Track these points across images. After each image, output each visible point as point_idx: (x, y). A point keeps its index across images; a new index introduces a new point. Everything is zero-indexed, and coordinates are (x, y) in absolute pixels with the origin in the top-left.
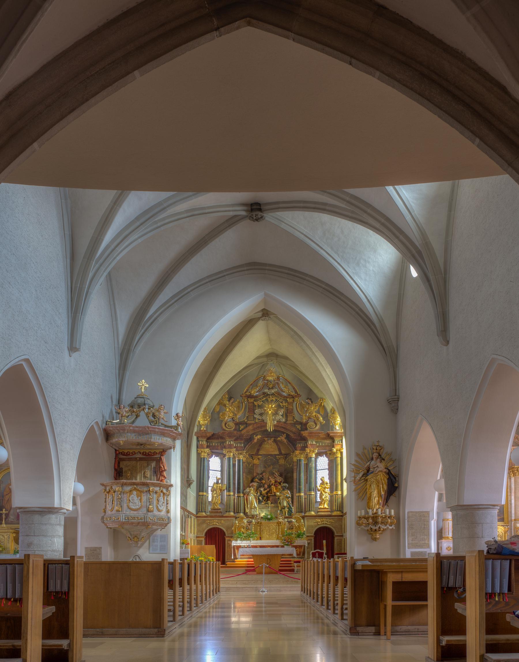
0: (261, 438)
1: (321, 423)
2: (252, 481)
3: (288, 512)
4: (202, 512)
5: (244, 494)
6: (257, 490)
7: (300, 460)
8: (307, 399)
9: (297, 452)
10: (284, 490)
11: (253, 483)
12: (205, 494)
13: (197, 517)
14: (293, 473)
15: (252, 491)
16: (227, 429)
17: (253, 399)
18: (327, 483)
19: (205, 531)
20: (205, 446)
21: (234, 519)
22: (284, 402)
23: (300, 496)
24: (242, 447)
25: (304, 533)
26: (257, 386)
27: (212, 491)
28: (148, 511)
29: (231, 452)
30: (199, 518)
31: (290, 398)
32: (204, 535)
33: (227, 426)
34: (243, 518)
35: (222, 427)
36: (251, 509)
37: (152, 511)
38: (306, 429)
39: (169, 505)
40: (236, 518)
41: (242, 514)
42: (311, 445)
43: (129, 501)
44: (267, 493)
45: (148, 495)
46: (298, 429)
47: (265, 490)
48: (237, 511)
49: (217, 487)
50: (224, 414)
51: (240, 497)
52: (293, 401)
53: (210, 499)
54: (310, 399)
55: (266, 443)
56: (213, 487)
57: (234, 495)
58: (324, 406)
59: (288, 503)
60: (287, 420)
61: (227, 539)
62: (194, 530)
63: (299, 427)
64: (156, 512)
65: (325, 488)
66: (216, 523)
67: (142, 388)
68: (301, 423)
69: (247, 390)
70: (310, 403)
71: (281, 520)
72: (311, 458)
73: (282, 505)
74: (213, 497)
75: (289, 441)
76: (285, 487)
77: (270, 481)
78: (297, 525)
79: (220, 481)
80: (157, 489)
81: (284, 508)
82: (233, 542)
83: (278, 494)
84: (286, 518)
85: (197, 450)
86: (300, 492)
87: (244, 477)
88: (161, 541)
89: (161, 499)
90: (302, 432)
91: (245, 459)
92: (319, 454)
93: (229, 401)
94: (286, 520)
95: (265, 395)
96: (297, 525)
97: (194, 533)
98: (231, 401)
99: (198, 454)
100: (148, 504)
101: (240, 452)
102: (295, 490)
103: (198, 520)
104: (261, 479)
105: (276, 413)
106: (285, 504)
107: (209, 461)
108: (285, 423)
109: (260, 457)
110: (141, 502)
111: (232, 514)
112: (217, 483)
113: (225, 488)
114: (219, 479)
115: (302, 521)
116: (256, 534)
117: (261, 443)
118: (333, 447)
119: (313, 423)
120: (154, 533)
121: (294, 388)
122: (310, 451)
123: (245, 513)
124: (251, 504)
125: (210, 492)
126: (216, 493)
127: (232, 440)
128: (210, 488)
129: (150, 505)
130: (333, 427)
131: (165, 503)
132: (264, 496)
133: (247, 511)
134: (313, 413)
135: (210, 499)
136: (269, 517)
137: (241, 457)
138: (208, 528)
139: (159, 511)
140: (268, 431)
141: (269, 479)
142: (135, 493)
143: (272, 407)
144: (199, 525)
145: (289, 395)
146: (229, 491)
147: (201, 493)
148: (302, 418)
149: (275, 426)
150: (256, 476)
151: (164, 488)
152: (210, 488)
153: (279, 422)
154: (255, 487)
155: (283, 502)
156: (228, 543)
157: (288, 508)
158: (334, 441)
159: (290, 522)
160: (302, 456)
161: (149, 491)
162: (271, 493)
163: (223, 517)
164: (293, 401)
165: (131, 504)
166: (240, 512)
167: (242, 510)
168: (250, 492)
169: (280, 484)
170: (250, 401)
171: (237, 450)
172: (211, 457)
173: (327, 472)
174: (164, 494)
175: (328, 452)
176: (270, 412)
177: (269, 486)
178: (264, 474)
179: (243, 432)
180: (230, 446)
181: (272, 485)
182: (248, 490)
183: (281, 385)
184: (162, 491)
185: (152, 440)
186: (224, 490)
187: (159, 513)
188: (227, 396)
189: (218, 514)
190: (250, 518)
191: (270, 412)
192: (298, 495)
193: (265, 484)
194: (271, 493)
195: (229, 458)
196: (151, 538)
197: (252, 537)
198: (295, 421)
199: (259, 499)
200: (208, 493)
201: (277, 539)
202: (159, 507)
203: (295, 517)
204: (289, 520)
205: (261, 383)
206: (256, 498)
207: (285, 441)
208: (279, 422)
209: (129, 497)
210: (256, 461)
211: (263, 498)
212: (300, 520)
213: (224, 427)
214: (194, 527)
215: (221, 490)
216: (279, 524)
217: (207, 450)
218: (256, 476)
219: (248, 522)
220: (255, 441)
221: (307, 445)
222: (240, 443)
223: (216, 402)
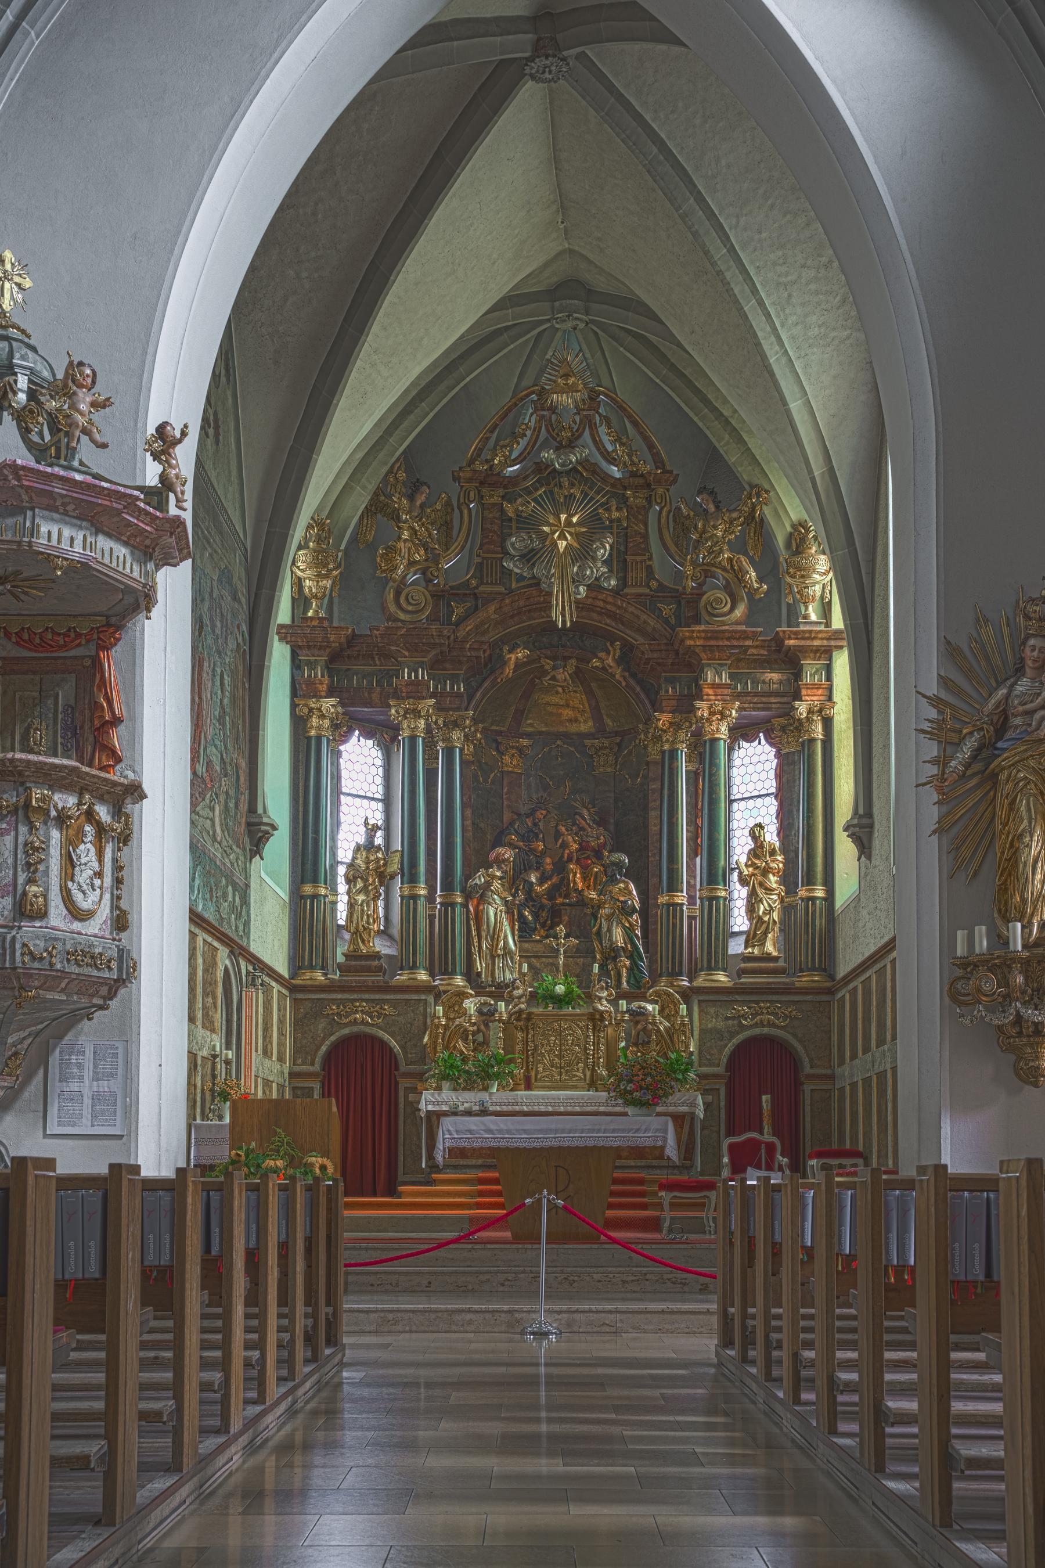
0: (530, 661)
1: (751, 593)
2: (497, 843)
3: (630, 970)
4: (312, 967)
5: (467, 896)
6: (514, 881)
7: (673, 753)
8: (699, 493)
9: (663, 719)
10: (613, 880)
11: (501, 850)
12: (323, 891)
13: (293, 989)
14: (646, 809)
15: (496, 885)
16: (402, 616)
17: (501, 491)
18: (773, 853)
19: (324, 1048)
20: (323, 688)
21: (431, 999)
22: (614, 503)
23: (675, 905)
24: (459, 695)
25: (690, 1063)
26: (515, 437)
27: (349, 881)
29: (417, 714)
30: (299, 996)
31: (636, 488)
32: (317, 1067)
33: (402, 599)
34: (462, 995)
35: (384, 608)
36: (493, 958)
38: (697, 620)
40: (438, 996)
41: (459, 981)
42: (714, 686)
44: (551, 894)
46: (666, 621)
47: (542, 881)
48: (441, 966)
49: (368, 862)
50: (392, 550)
51: (453, 905)
52: (649, 500)
53: (342, 918)
54: (712, 493)
55: (546, 681)
56: (351, 866)
57: (431, 898)
58: (762, 521)
59: (629, 932)
60: (623, 582)
61: (403, 1084)
62: (281, 1045)
63: (667, 610)
65: (766, 872)
66: (364, 1018)
68: (676, 596)
69: (479, 451)
70: (712, 508)
71: (604, 1006)
72: (714, 741)
73: (606, 943)
74: (351, 905)
75: (633, 675)
76: (619, 865)
77: (565, 845)
78: (664, 1025)
79: (379, 840)
81: (612, 954)
82: (426, 1096)
83: (593, 895)
84: (621, 996)
85: (294, 706)
86: (673, 887)
87: (468, 823)
90: (684, 631)
91: (469, 749)
92: (743, 732)
93: (411, 498)
94: (623, 1003)
95: (545, 474)
96: (664, 1025)
97: (281, 1059)
98: (420, 500)
99: (299, 723)
101: (453, 715)
102: (653, 881)
103: (295, 1002)
104: (530, 836)
105: (583, 553)
106: (618, 936)
107: (338, 754)
108: (617, 592)
109: (525, 742)
111: (423, 976)
112: (369, 846)
113: (395, 867)
114: (375, 828)
115: (683, 1008)
116: (511, 1061)
117: (530, 678)
118: (797, 697)
119: (721, 595)
121: (651, 446)
122: (712, 713)
123: (470, 975)
124: (494, 937)
125: (342, 887)
126: (365, 890)
127: (421, 665)
128: (342, 870)
130: (794, 614)
132: (542, 907)
133: (480, 966)
134: (721, 551)
135: (342, 918)
136: (560, 989)
137: (457, 735)
138: (333, 1038)
140: (555, 623)
141: (558, 834)
143: (569, 523)
144: (298, 1023)
145: (633, 475)
146: (412, 879)
147: (308, 889)
148: (679, 576)
149: (581, 606)
150: (512, 824)
152: (342, 870)
153: (594, 587)
154: (508, 868)
155: (609, 930)
156: (407, 1102)
157: (630, 957)
158: (797, 674)
159: (638, 1015)
160: (682, 735)
162: (567, 896)
163: (387, 989)
164: (649, 500)
166: (454, 972)
167: (460, 965)
168: (488, 884)
169: (598, 854)
170: (488, 500)
171: (439, 708)
172: (344, 739)
173: (771, 805)
175: (776, 722)
176: (562, 545)
177: (561, 867)
178: (540, 814)
179: (461, 634)
180: (416, 691)
181: (570, 859)
182: (480, 879)
183: (603, 430)
186: (392, 877)
188: (402, 475)
189: (370, 979)
190: (491, 995)
191: (562, 545)
192: (663, 899)
193: (543, 853)
194: (567, 896)
195: (413, 739)
197: (497, 1076)
198: (654, 584)
199: (522, 918)
200: (334, 891)
201: (592, 1085)
203: (657, 994)
204: (635, 1005)
205: (530, 418)
206: (509, 912)
207: (618, 672)
208: (594, 587)
210: (511, 762)
211: (536, 916)
212: (676, 1005)
213: (392, 608)
214: (281, 1033)
215: (381, 876)
216: (596, 1019)
217: (328, 704)
218: (512, 824)
219: (480, 1011)
220: (509, 670)
221: (699, 689)
222: (455, 679)
223: (360, 500)
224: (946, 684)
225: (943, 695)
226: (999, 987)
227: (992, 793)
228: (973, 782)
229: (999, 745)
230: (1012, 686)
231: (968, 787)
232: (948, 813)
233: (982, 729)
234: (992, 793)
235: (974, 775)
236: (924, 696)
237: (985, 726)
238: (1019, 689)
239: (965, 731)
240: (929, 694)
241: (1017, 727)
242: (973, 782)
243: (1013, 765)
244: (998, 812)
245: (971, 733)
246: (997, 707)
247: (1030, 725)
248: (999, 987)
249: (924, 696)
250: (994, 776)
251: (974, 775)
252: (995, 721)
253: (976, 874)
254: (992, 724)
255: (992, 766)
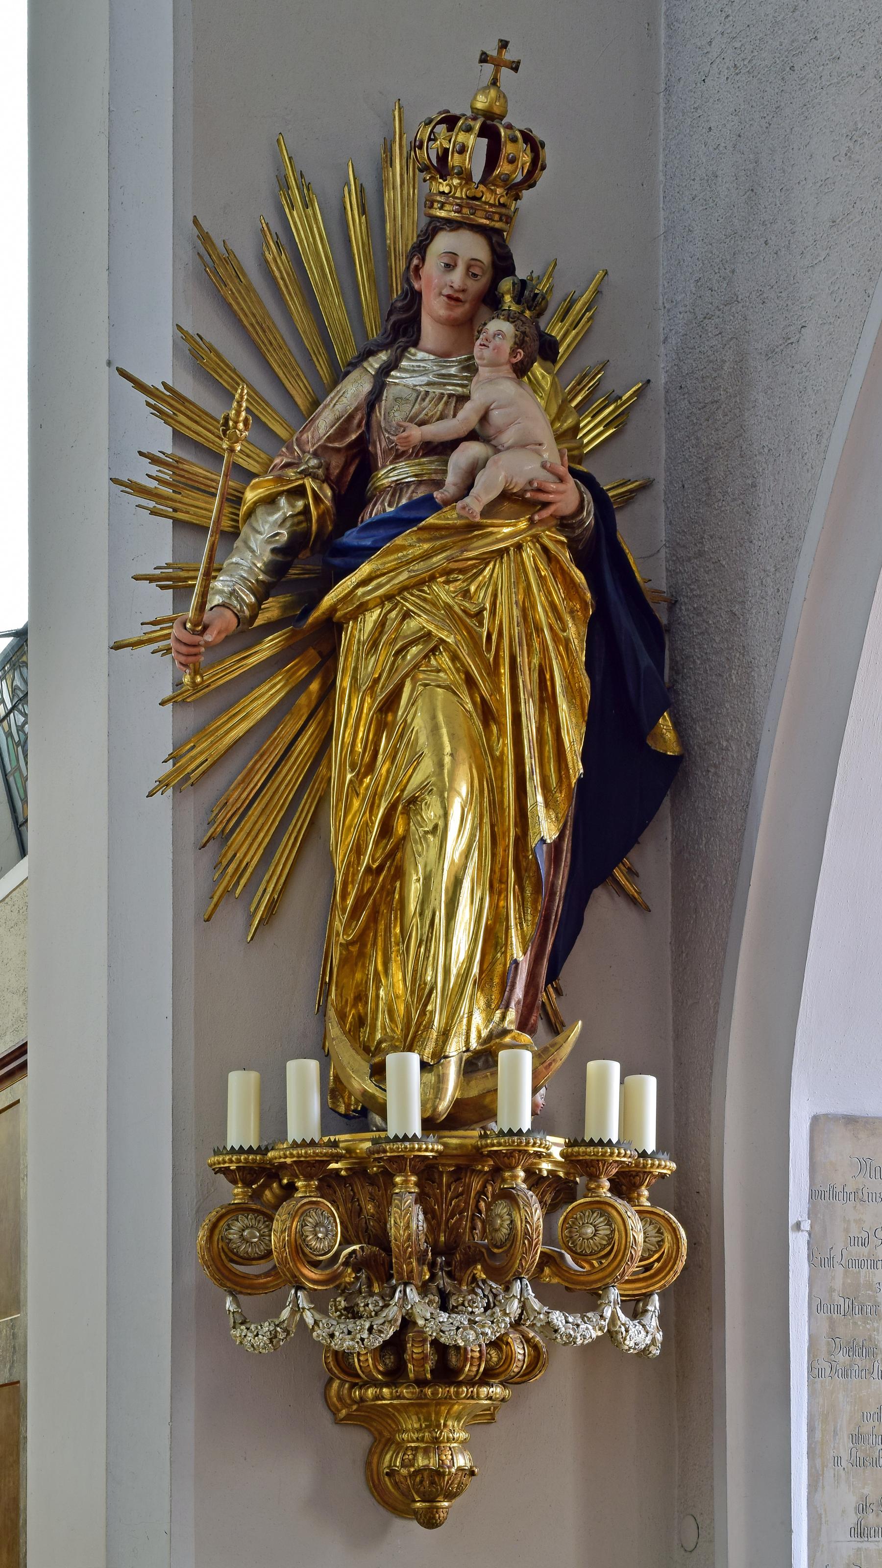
224: (195, 355)
225: (189, 387)
226: (346, 1241)
227: (315, 686)
228: (268, 647)
229: (351, 538)
230: (385, 370)
231: (253, 660)
232: (201, 732)
233: (299, 492)
234: (315, 686)
235: (270, 627)
236: (139, 385)
237: (309, 483)
238: (403, 380)
239: (250, 496)
240: (152, 380)
241: (399, 487)
242: (268, 647)
243: (389, 597)
244: (343, 735)
245: (270, 501)
246: (342, 432)
247: (439, 484)
248: (346, 1241)
249: (139, 385)
250: (332, 628)
251: (270, 627)
252: (335, 472)
253: (273, 908)
254: (327, 479)
255: (328, 600)
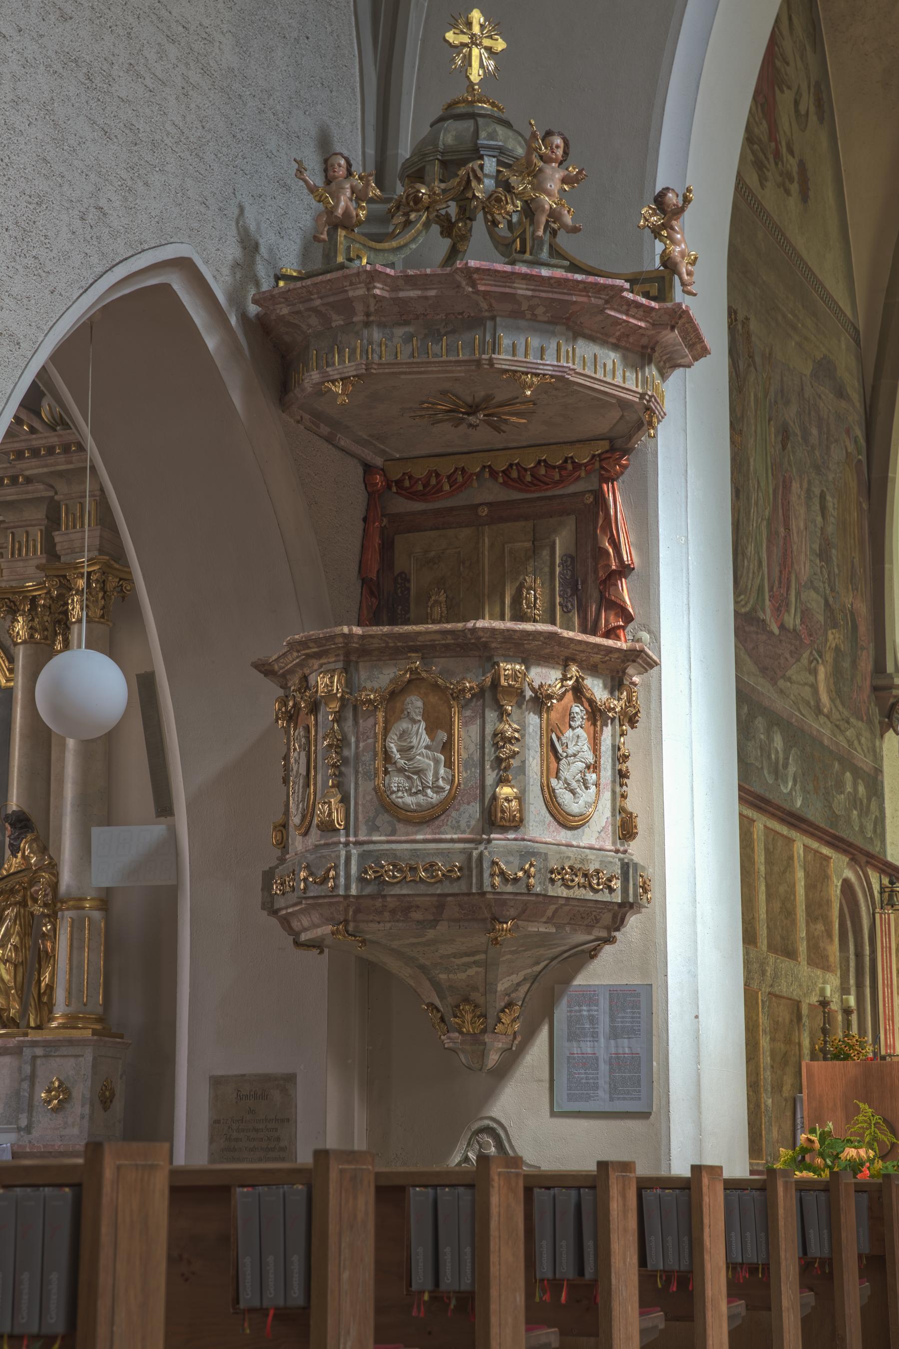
28: (494, 819)
37: (516, 823)
39: (633, 786)
43: (387, 757)
45: (491, 715)
64: (540, 829)
67: (468, 59)
80: (546, 677)
88: (614, 1034)
89: (577, 740)
100: (491, 777)
110: (449, 764)
120: (580, 980)
129: (502, 781)
131: (607, 773)
139: (566, 820)
142: (415, 703)
151: (594, 670)
161: (495, 683)
165: (396, 781)
174: (596, 715)
184: (578, 691)
185: (503, 359)
187: (564, 836)
196: (561, 1012)
202: (565, 797)
209: (386, 731)
